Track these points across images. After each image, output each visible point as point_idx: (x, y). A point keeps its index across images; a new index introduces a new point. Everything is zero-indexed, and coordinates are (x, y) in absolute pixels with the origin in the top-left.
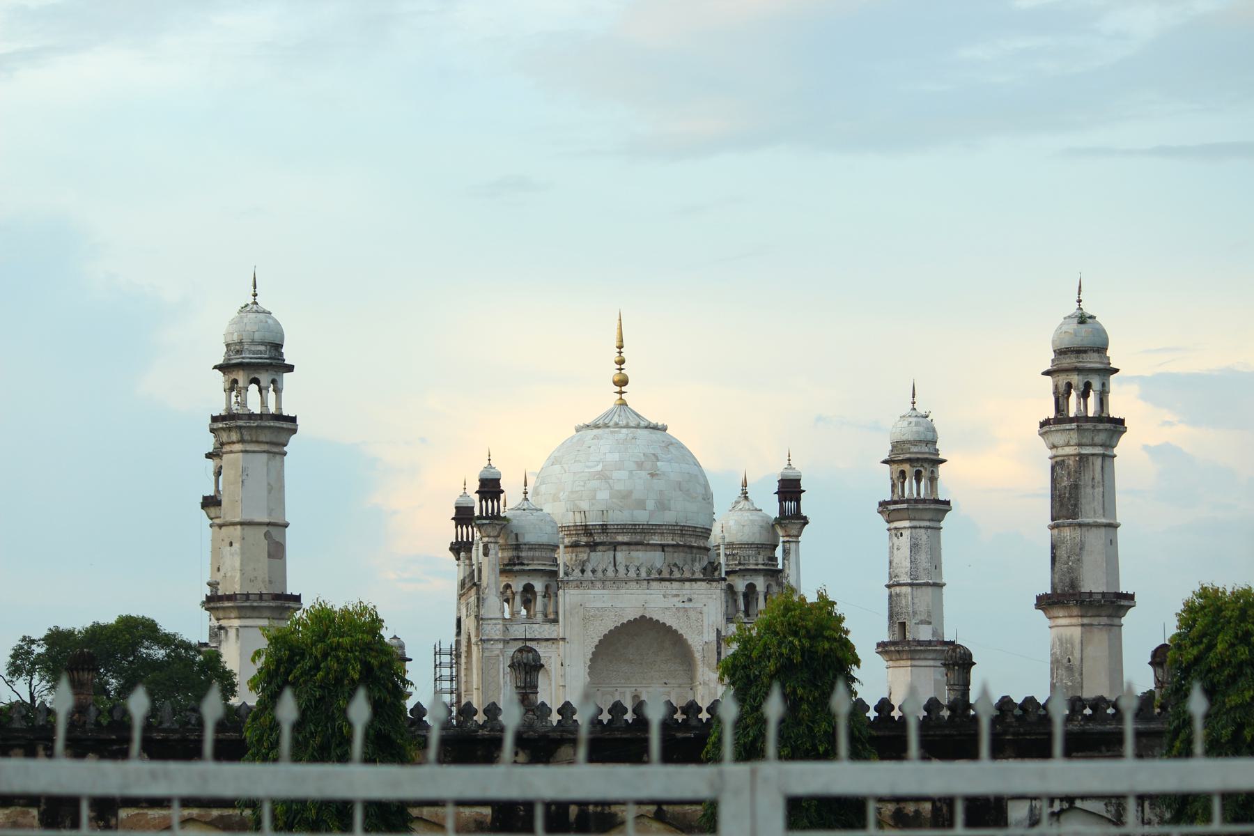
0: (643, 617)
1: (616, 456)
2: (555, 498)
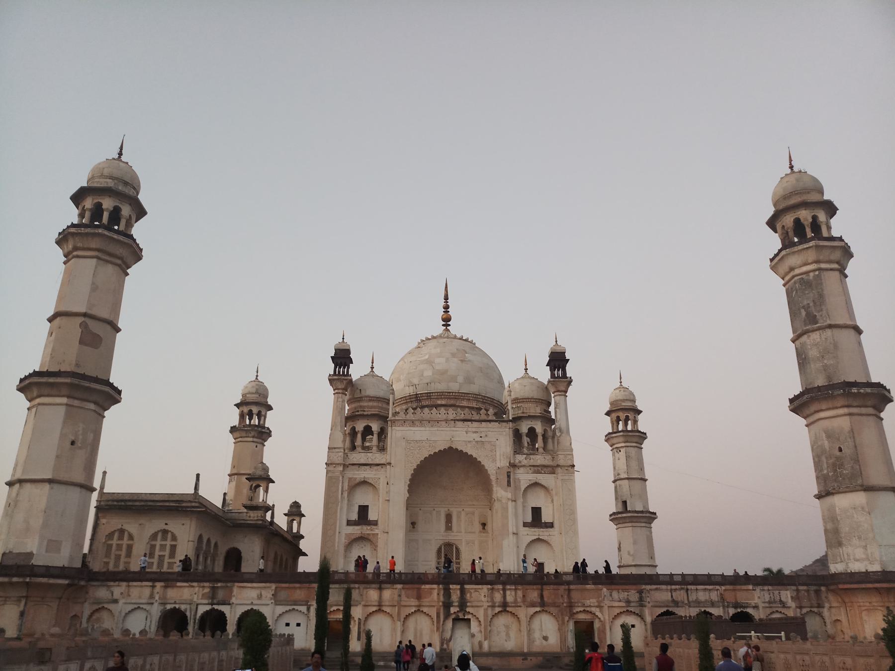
0: (451, 448)
1: (438, 350)
2: (399, 380)
